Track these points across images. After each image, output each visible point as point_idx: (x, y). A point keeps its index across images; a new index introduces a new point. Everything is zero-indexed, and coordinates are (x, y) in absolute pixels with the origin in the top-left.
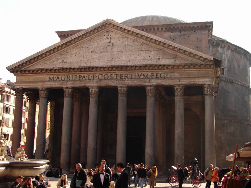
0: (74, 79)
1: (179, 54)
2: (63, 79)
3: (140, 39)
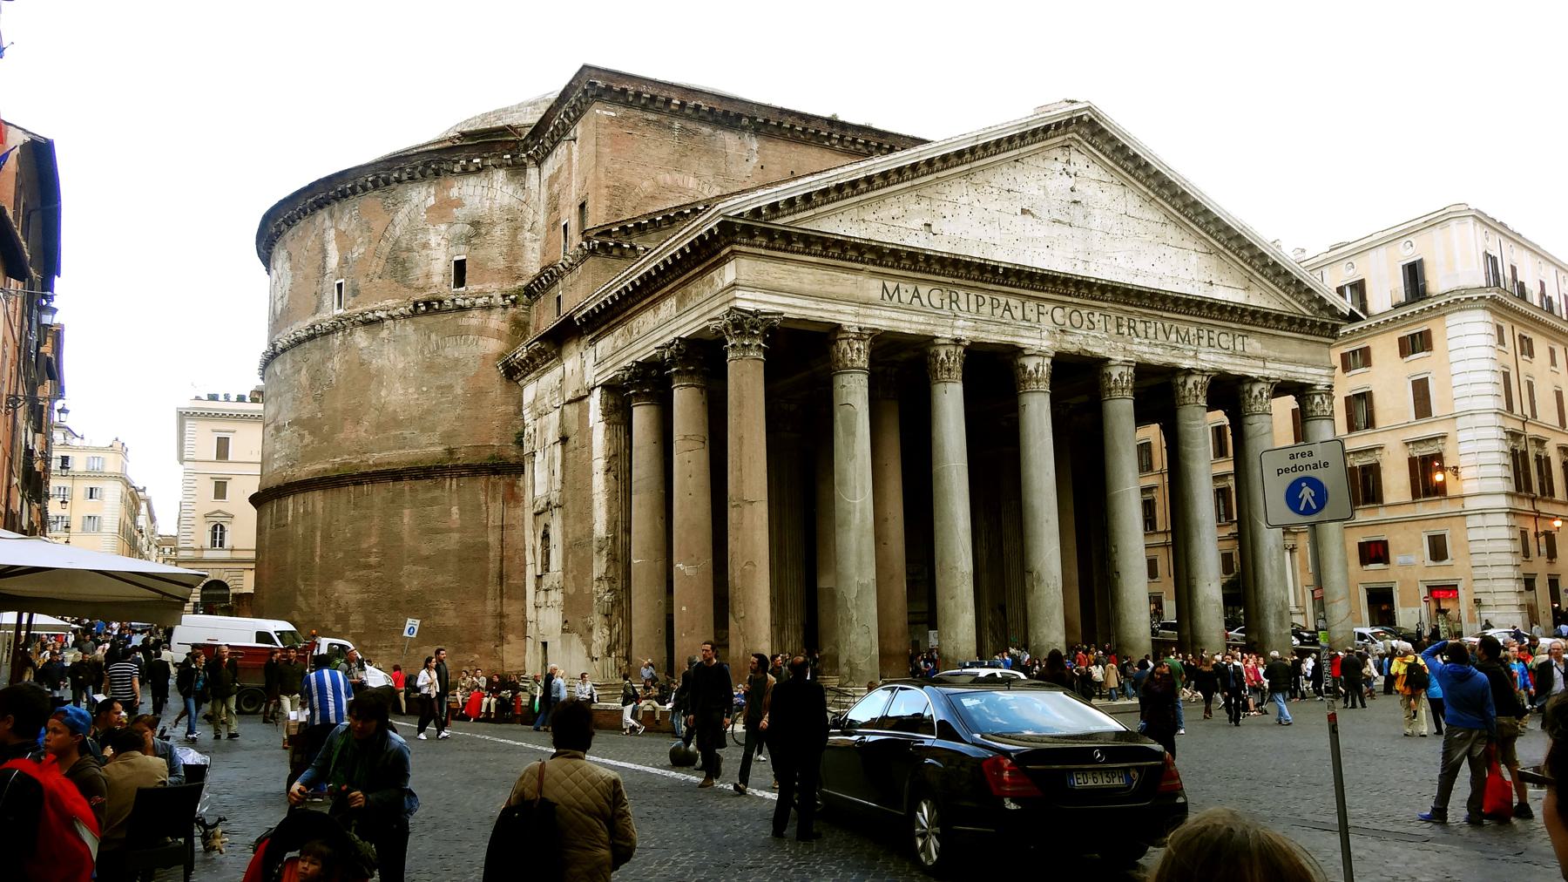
0: (973, 307)
2: (936, 302)
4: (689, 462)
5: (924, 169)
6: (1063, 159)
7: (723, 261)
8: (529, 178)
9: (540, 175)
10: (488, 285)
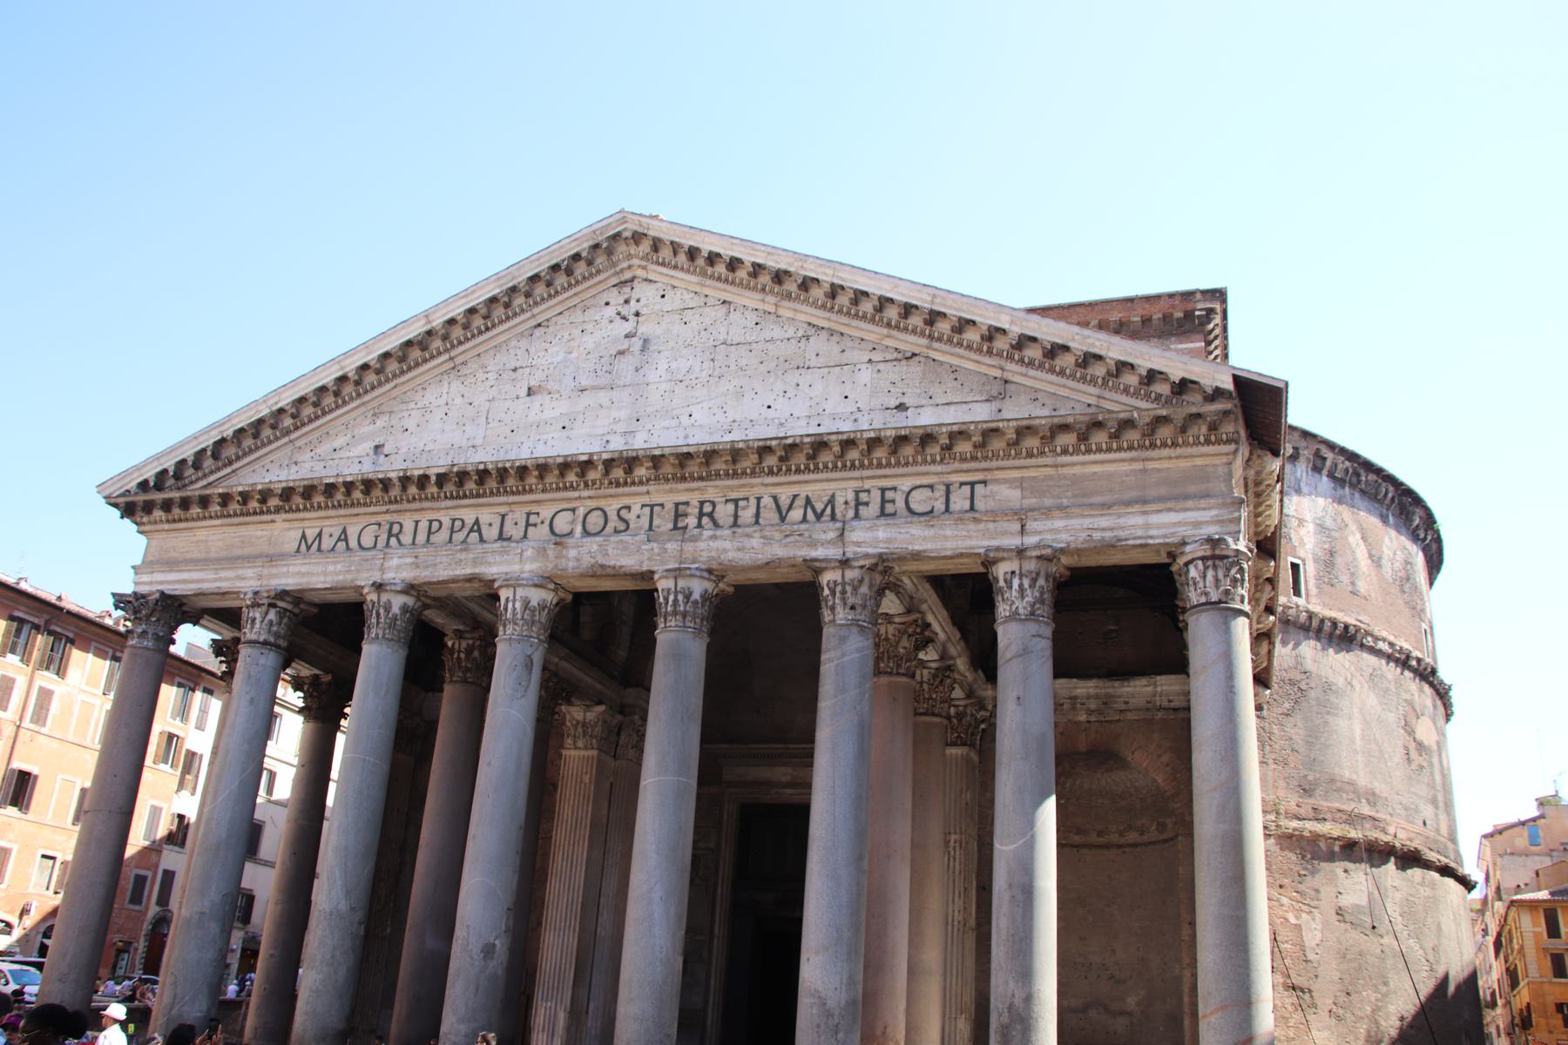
0: (422, 537)
1: (1023, 370)
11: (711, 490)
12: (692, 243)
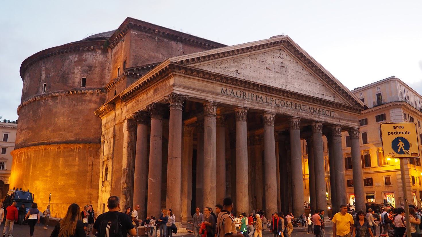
0: (250, 97)
3: (309, 69)
4: (155, 144)
5: (236, 52)
6: (279, 53)
7: (170, 78)
8: (108, 54)
9: (112, 52)
10: (93, 86)
11: (301, 103)
12: (298, 49)
